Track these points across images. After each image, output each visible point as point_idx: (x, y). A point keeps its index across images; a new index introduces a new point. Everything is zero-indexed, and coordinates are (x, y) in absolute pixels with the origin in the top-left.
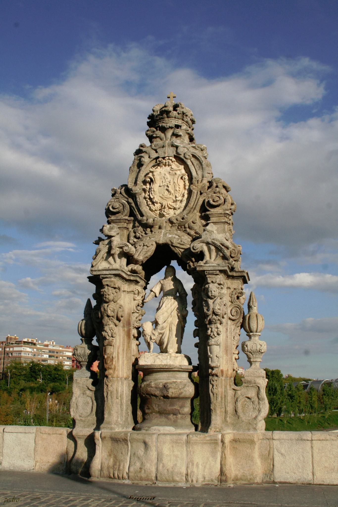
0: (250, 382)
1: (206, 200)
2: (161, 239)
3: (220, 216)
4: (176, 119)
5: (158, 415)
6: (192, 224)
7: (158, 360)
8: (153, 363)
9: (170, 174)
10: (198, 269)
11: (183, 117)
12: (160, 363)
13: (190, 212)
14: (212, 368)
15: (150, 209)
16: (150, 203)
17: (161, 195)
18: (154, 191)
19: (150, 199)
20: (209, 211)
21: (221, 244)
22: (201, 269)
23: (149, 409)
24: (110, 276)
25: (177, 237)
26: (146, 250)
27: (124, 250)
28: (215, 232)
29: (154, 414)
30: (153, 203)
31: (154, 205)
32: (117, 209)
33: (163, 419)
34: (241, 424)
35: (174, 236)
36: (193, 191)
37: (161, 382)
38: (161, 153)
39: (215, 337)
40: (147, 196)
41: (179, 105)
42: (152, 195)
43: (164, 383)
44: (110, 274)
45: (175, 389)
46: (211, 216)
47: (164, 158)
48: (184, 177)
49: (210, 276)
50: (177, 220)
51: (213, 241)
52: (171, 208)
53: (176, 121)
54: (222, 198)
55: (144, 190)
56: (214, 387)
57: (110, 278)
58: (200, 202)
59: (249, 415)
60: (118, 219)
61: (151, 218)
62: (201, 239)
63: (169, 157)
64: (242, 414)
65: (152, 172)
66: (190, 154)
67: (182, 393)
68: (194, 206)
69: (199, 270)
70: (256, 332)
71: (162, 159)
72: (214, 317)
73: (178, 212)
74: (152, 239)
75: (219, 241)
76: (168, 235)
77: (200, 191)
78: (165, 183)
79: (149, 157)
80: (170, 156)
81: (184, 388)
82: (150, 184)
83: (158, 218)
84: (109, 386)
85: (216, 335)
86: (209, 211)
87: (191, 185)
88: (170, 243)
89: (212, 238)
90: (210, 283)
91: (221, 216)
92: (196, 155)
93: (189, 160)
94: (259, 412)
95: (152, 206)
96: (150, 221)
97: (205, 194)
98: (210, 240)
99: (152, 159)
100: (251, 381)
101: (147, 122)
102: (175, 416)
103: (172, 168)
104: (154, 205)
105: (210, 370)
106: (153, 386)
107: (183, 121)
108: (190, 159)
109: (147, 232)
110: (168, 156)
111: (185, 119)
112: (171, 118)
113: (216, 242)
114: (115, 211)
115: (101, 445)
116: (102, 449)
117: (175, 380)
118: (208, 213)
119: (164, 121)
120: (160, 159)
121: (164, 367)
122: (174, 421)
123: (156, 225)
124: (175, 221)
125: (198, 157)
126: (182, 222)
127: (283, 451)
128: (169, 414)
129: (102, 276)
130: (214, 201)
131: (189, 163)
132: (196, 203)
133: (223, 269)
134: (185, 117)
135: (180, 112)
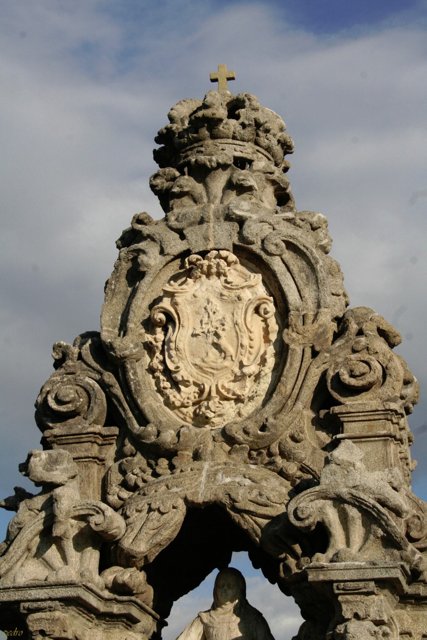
1: (331, 373)
3: (372, 418)
6: (291, 443)
9: (222, 300)
10: (311, 577)
11: (258, 135)
13: (283, 407)
15: (168, 403)
16: (168, 385)
17: (198, 361)
18: (177, 349)
19: (167, 372)
20: (339, 404)
21: (379, 501)
22: (321, 577)
24: (49, 603)
25: (248, 482)
26: (157, 524)
27: (93, 526)
28: (358, 464)
30: (175, 384)
31: (179, 390)
32: (70, 405)
35: (238, 480)
36: (292, 346)
40: (156, 363)
41: (244, 101)
42: (173, 362)
44: (50, 599)
46: (346, 419)
47: (204, 254)
48: (263, 306)
49: (349, 597)
50: (246, 432)
51: (354, 492)
52: (227, 399)
53: (238, 148)
54: (375, 364)
55: (149, 348)
57: (51, 609)
60: (73, 431)
61: (170, 427)
62: (317, 488)
63: (218, 250)
65: (171, 295)
66: (278, 241)
68: (296, 391)
69: (316, 579)
71: (199, 257)
73: (248, 409)
74: (175, 490)
75: (373, 493)
76: (220, 476)
77: (313, 348)
78: (209, 326)
79: (162, 252)
80: (221, 247)
82: (166, 330)
83: (190, 429)
86: (339, 404)
88: (226, 501)
89: (351, 484)
90: (348, 620)
91: (376, 417)
92: (298, 244)
93: (278, 259)
95: (171, 393)
96: (169, 436)
97: (328, 355)
98: (344, 491)
99: (169, 258)
101: (155, 152)
103: (228, 283)
104: (179, 390)
107: (258, 148)
108: (280, 256)
109: (159, 470)
111: (264, 141)
112: (223, 138)
113: (362, 496)
114: (65, 410)
118: (337, 409)
120: (194, 257)
123: (186, 450)
124: (240, 436)
125: (302, 248)
129: (27, 605)
130: (352, 376)
131: (277, 265)
132: (299, 383)
133: (387, 576)
134: (261, 134)
135: (247, 122)
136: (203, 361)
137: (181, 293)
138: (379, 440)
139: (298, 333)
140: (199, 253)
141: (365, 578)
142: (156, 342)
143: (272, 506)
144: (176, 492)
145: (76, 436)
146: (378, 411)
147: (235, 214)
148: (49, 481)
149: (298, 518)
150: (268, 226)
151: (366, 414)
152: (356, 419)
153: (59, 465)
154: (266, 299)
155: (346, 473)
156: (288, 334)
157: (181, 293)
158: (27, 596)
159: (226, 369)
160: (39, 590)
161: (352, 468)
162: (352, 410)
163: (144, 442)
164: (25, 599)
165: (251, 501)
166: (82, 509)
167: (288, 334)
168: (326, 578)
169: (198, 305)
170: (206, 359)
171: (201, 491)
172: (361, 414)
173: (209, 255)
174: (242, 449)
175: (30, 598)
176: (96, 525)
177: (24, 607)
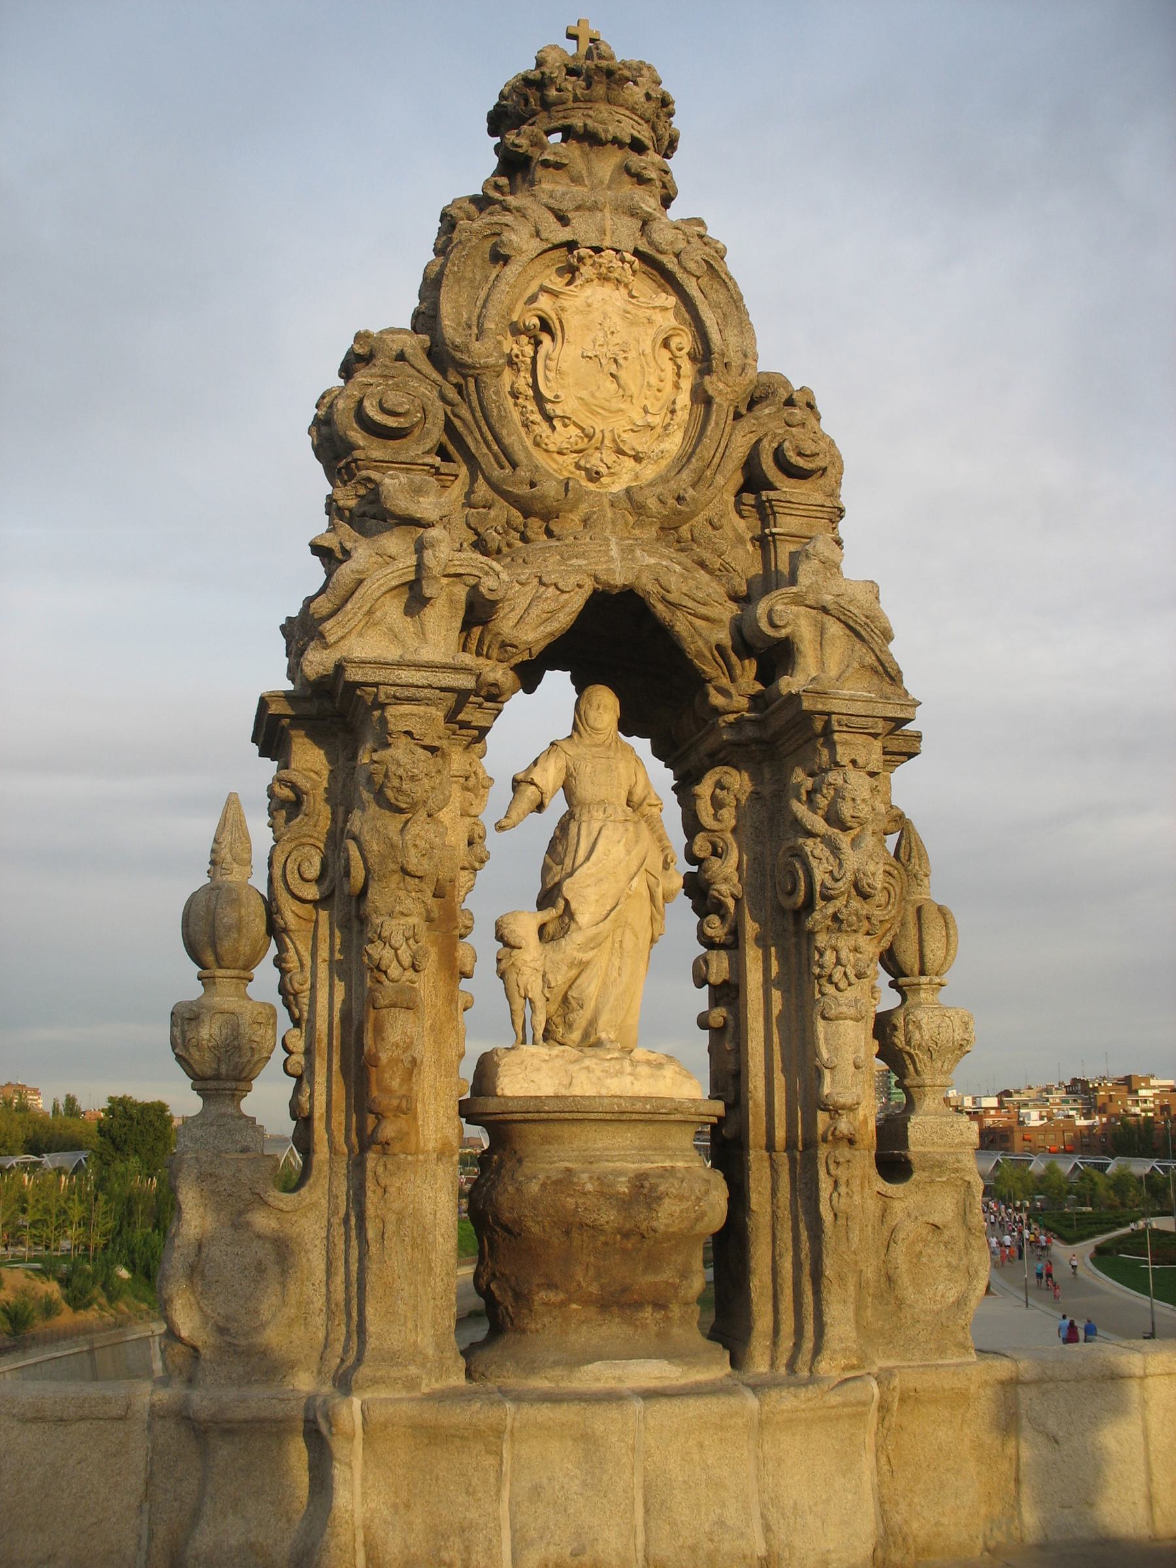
0: (938, 1165)
2: (617, 566)
4: (636, 118)
5: (592, 1311)
7: (583, 1076)
8: (563, 1092)
9: (624, 318)
12: (590, 1091)
14: (835, 1111)
16: (537, 417)
17: (584, 394)
18: (558, 371)
19: (539, 398)
20: (772, 488)
23: (551, 1286)
25: (678, 568)
26: (553, 606)
27: (483, 590)
29: (574, 1306)
33: (614, 1329)
34: (912, 1332)
35: (664, 563)
36: (717, 400)
37: (620, 1173)
38: (582, 229)
39: (850, 984)
43: (632, 1175)
44: (430, 687)
45: (681, 1198)
46: (781, 510)
47: (598, 250)
49: (846, 736)
52: (624, 453)
55: (511, 362)
56: (843, 1189)
57: (428, 702)
59: (935, 1294)
62: (794, 589)
63: (617, 251)
64: (910, 1290)
65: (554, 294)
66: (699, 258)
67: (703, 1215)
68: (716, 460)
70: (922, 972)
71: (592, 253)
72: (856, 903)
73: (649, 472)
74: (574, 561)
75: (861, 607)
76: (638, 553)
78: (604, 349)
81: (707, 1192)
82: (538, 343)
84: (392, 1190)
85: (853, 978)
86: (772, 488)
87: (707, 377)
88: (652, 587)
92: (720, 270)
93: (695, 279)
94: (970, 1283)
95: (543, 428)
96: (550, 489)
97: (755, 422)
98: (828, 599)
99: (546, 246)
100: (945, 1162)
102: (659, 1315)
103: (633, 297)
104: (553, 428)
105: (822, 1118)
106: (589, 1187)
108: (698, 278)
110: (616, 246)
112: (622, 106)
114: (395, 425)
115: (358, 1463)
116: (364, 1479)
117: (667, 1164)
118: (772, 494)
119: (591, 113)
121: (638, 1106)
122: (658, 1335)
123: (571, 511)
124: (652, 504)
125: (724, 276)
126: (680, 513)
127: (1052, 1425)
128: (638, 1305)
130: (800, 454)
132: (721, 450)
135: (653, 95)
136: (593, 396)
137: (569, 295)
140: (592, 248)
141: (875, 714)
142: (523, 356)
143: (712, 606)
144: (579, 566)
146: (823, 506)
147: (641, 208)
148: (418, 516)
149: (773, 625)
150: (681, 236)
151: (807, 507)
153: (422, 496)
154: (681, 330)
155: (829, 575)
156: (711, 382)
157: (569, 295)
158: (393, 677)
160: (413, 672)
161: (836, 570)
162: (793, 500)
164: (391, 682)
165: (685, 595)
166: (461, 565)
167: (711, 382)
168: (826, 709)
169: (591, 317)
170: (597, 394)
171: (618, 570)
173: (602, 254)
174: (651, 524)
175: (398, 681)
177: (386, 693)
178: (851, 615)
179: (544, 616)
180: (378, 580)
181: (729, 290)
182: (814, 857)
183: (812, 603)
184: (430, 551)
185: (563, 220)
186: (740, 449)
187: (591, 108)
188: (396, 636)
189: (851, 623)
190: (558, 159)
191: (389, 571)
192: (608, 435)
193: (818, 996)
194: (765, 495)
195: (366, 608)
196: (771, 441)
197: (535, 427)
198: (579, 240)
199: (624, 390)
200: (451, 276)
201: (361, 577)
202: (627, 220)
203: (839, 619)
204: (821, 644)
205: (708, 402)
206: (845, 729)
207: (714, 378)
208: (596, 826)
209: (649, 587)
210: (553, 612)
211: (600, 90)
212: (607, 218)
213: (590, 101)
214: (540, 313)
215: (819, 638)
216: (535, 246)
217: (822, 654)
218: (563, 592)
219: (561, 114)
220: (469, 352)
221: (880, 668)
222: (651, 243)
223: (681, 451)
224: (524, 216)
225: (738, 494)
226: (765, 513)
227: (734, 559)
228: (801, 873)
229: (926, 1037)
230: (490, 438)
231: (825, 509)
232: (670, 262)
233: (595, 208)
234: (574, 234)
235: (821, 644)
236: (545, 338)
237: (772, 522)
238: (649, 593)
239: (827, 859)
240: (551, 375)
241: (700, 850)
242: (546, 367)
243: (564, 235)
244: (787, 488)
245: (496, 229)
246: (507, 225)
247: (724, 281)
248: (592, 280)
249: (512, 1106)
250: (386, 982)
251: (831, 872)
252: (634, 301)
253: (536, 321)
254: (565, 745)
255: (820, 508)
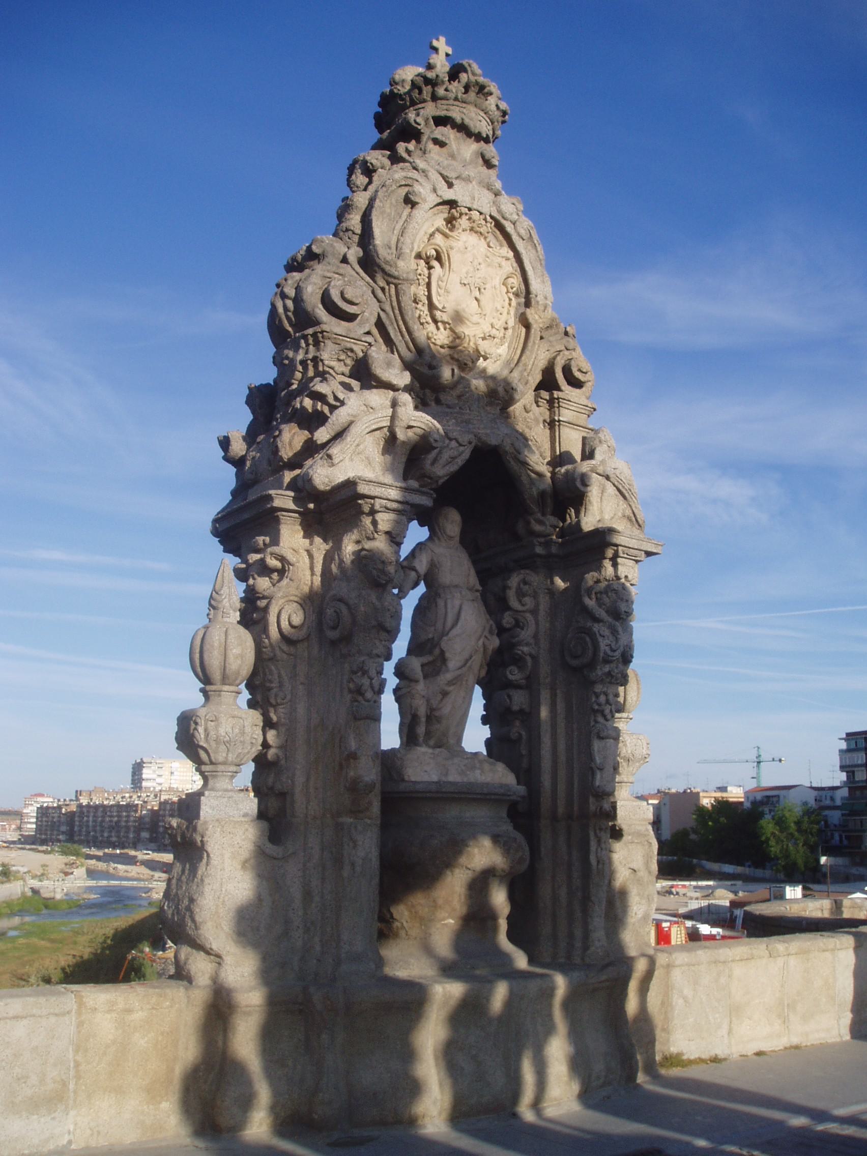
19: (431, 306)
26: (456, 453)
31: (438, 329)
38: (457, 193)
46: (564, 405)
58: (542, 363)
86: (559, 389)
88: (508, 448)
91: (583, 411)
99: (439, 200)
104: (438, 329)
110: (480, 209)
118: (561, 394)
130: (580, 370)
137: (456, 239)
138: (583, 431)
139: (540, 317)
143: (540, 465)
145: (352, 341)
146: (587, 406)
147: (495, 186)
151: (578, 405)
152: (571, 408)
158: (386, 493)
159: (477, 325)
162: (571, 400)
163: (417, 370)
164: (384, 497)
166: (414, 420)
167: (531, 314)
172: (575, 405)
174: (498, 405)
175: (389, 497)
176: (436, 441)
178: (622, 482)
179: (450, 460)
180: (366, 423)
181: (537, 251)
182: (600, 635)
183: (601, 472)
184: (403, 409)
185: (450, 185)
186: (542, 361)
187: (464, 108)
188: (370, 463)
189: (621, 487)
190: (444, 139)
191: (373, 418)
192: (472, 339)
193: (592, 723)
194: (556, 394)
195: (356, 442)
196: (561, 359)
197: (427, 326)
198: (459, 200)
199: (482, 310)
200: (378, 208)
201: (352, 419)
202: (486, 192)
203: (614, 485)
204: (601, 498)
205: (527, 326)
206: (625, 556)
207: (533, 311)
208: (457, 603)
209: (507, 448)
210: (453, 458)
211: (472, 95)
212: (474, 186)
213: (465, 103)
214: (437, 248)
215: (600, 495)
216: (435, 200)
217: (601, 505)
218: (461, 445)
219: (445, 107)
220: (396, 267)
221: (634, 519)
222: (499, 211)
223: (509, 357)
224: (426, 176)
225: (537, 389)
226: (552, 403)
227: (536, 434)
228: (590, 645)
229: (629, 752)
230: (404, 329)
231: (587, 408)
232: (509, 228)
233: (468, 180)
234: (456, 196)
235: (601, 498)
236: (435, 263)
237: (557, 412)
238: (507, 452)
239: (608, 637)
240: (441, 292)
241: (507, 623)
242: (439, 286)
243: (449, 195)
244: (568, 391)
245: (409, 182)
246: (417, 181)
247: (535, 245)
248: (466, 230)
249: (418, 787)
250: (363, 702)
251: (610, 645)
252: (490, 249)
253: (434, 253)
254: (430, 544)
255: (585, 407)
